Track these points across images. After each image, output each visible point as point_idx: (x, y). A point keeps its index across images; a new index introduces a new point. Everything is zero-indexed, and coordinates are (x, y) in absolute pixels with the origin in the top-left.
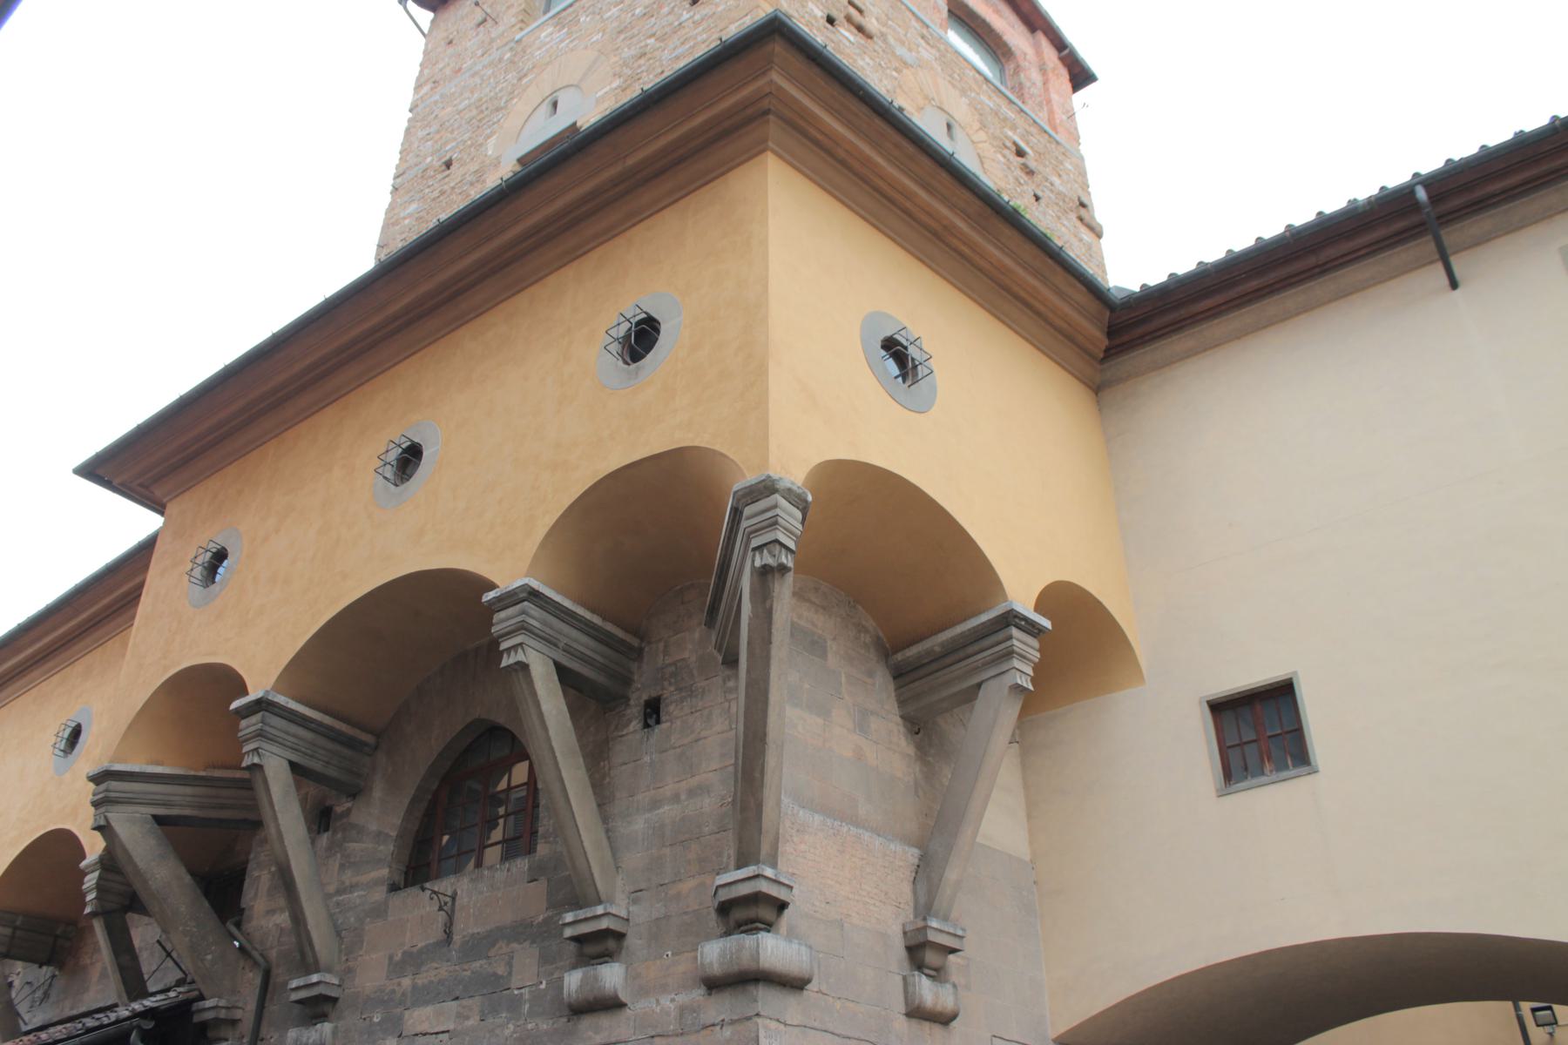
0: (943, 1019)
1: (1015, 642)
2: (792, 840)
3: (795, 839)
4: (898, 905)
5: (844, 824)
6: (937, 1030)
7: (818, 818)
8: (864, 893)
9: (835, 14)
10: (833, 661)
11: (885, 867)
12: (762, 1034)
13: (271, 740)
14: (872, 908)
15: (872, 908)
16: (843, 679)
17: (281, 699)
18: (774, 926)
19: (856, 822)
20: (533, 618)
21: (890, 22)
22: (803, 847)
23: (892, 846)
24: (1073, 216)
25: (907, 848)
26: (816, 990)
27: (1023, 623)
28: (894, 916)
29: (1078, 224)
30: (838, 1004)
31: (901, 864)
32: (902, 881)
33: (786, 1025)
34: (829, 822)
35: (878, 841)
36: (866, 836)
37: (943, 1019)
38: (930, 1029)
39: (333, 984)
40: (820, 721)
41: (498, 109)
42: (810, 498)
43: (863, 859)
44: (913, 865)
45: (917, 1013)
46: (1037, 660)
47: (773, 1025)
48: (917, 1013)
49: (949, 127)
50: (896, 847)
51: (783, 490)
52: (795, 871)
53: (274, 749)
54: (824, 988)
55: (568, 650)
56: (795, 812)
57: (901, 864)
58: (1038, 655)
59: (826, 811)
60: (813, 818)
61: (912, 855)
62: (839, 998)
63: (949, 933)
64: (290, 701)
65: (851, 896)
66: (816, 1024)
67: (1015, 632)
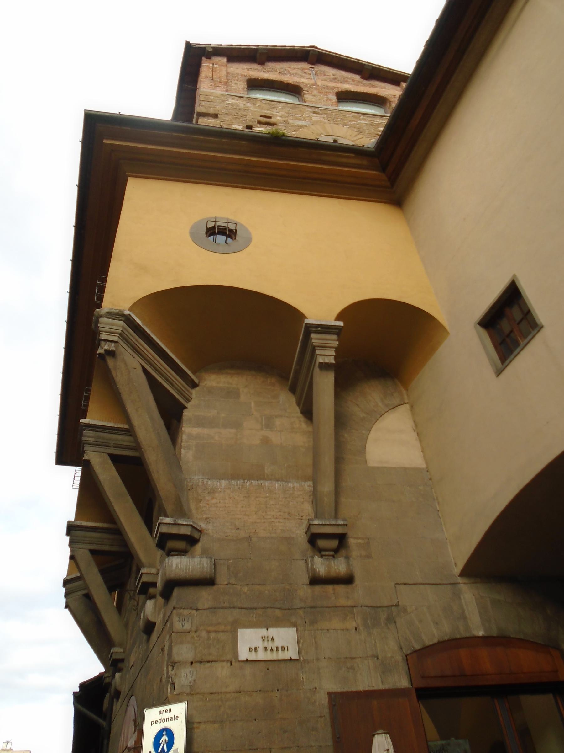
1: (313, 341)
2: (205, 499)
3: (207, 498)
4: (300, 518)
5: (246, 481)
6: (341, 589)
7: (224, 483)
8: (269, 517)
10: (243, 398)
11: (286, 498)
13: (77, 542)
14: (277, 524)
15: (277, 524)
16: (253, 404)
17: (78, 523)
18: (189, 553)
20: (89, 437)
22: (214, 501)
23: (290, 485)
25: (303, 483)
26: (226, 583)
27: (319, 329)
28: (297, 525)
30: (245, 589)
31: (299, 493)
32: (303, 503)
33: (197, 609)
34: (234, 482)
35: (277, 485)
36: (267, 483)
38: (334, 589)
39: (121, 652)
40: (233, 431)
42: (127, 312)
43: (266, 497)
44: (310, 492)
45: (316, 580)
46: (337, 346)
47: (186, 612)
48: (316, 580)
50: (293, 484)
51: (105, 314)
52: (208, 516)
53: (81, 546)
54: (233, 581)
55: (117, 446)
56: (205, 483)
57: (299, 493)
58: (337, 343)
60: (220, 483)
61: (308, 486)
62: (247, 585)
63: (330, 525)
64: (81, 522)
65: (258, 521)
66: (226, 604)
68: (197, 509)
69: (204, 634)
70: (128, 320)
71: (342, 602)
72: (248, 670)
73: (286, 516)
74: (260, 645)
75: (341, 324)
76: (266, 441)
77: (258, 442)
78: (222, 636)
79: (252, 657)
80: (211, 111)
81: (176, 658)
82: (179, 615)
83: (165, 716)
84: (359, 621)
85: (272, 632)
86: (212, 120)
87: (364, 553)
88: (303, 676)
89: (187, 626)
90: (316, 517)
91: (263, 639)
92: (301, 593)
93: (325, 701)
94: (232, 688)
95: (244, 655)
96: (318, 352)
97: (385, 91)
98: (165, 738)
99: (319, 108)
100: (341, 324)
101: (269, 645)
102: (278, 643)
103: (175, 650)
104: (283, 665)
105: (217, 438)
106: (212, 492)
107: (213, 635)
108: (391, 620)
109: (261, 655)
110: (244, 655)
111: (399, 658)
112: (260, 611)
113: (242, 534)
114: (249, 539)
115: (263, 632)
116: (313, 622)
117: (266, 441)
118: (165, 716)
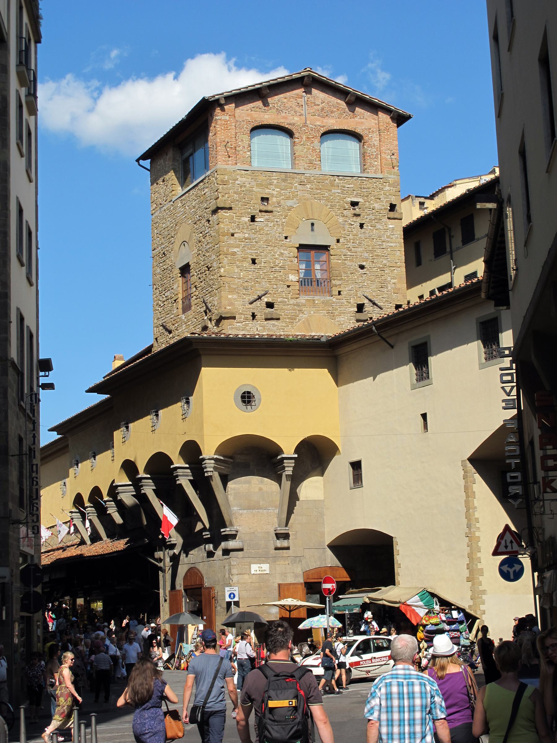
0: (288, 548)
9: (254, 212)
12: (231, 561)
19: (259, 508)
21: (283, 191)
23: (270, 511)
24: (385, 219)
29: (388, 220)
30: (253, 551)
34: (249, 511)
36: (261, 510)
37: (288, 548)
41: (172, 237)
42: (215, 457)
45: (277, 549)
47: (234, 559)
48: (277, 549)
49: (313, 224)
59: (249, 508)
67: (285, 461)
68: (236, 522)
69: (240, 566)
70: (216, 460)
71: (285, 555)
72: (254, 576)
73: (267, 523)
74: (258, 569)
75: (296, 456)
76: (261, 489)
77: (258, 490)
78: (246, 567)
79: (255, 573)
80: (227, 206)
81: (233, 573)
82: (232, 560)
83: (231, 590)
84: (290, 561)
85: (262, 565)
86: (227, 213)
87: (294, 537)
88: (270, 578)
89: (235, 564)
90: (279, 526)
91: (259, 567)
92: (271, 552)
93: (277, 585)
94: (249, 582)
95: (252, 573)
96: (286, 469)
97: (362, 123)
98: (232, 596)
99: (305, 175)
100: (296, 456)
101: (261, 569)
102: (263, 569)
103: (232, 571)
104: (264, 575)
105: (241, 489)
106: (241, 514)
107: (243, 566)
108: (300, 561)
109: (258, 572)
110: (252, 573)
111: (301, 573)
112: (258, 558)
113: (252, 531)
114: (254, 533)
115: (259, 565)
116: (275, 562)
117: (261, 489)
118: (231, 590)
